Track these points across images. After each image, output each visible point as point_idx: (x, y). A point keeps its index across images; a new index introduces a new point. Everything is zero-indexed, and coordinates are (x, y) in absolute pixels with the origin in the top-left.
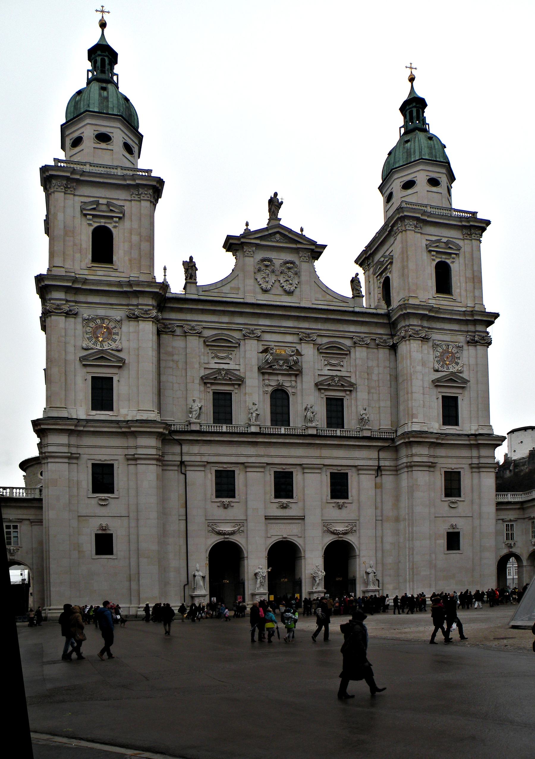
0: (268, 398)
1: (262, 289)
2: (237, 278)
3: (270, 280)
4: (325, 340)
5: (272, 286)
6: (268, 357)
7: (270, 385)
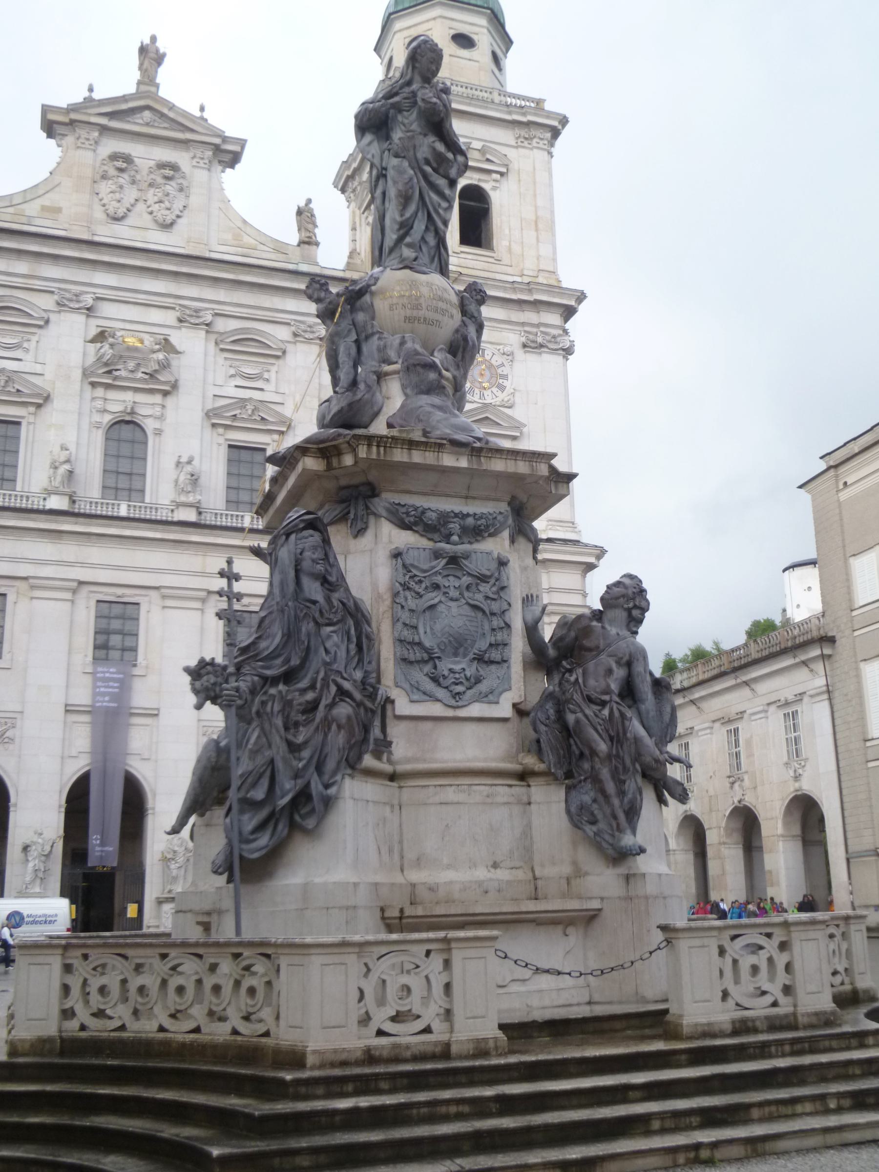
0: (99, 437)
1: (108, 215)
2: (57, 189)
3: (125, 198)
4: (234, 324)
5: (129, 210)
6: (102, 351)
7: (105, 411)
